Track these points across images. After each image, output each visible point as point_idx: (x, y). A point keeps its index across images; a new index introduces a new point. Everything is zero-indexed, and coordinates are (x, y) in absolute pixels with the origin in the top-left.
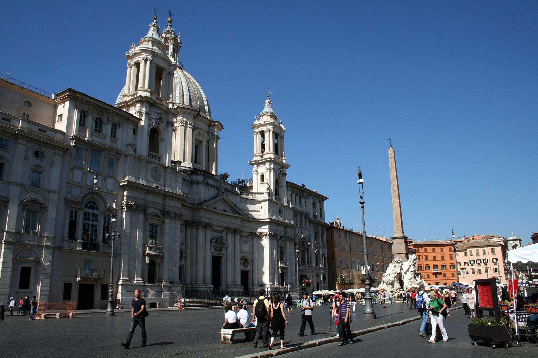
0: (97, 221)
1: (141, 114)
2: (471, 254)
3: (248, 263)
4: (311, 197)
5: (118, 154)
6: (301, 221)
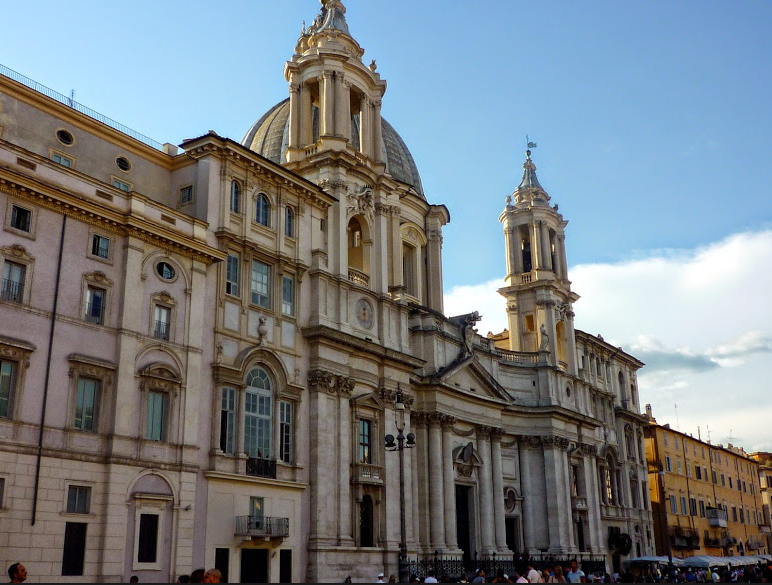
4: (615, 362)
5: (299, 268)
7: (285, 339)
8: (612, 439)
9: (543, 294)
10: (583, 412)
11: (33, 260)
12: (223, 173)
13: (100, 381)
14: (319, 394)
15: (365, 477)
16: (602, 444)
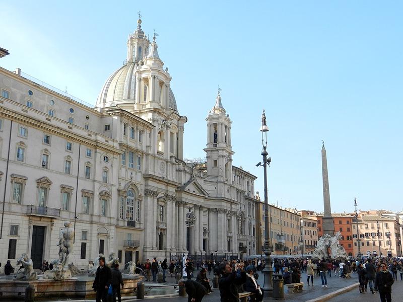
2: (367, 228)
5: (143, 153)
6: (240, 198)
8: (243, 209)
9: (221, 153)
12: (121, 121)
13: (89, 197)
15: (161, 226)
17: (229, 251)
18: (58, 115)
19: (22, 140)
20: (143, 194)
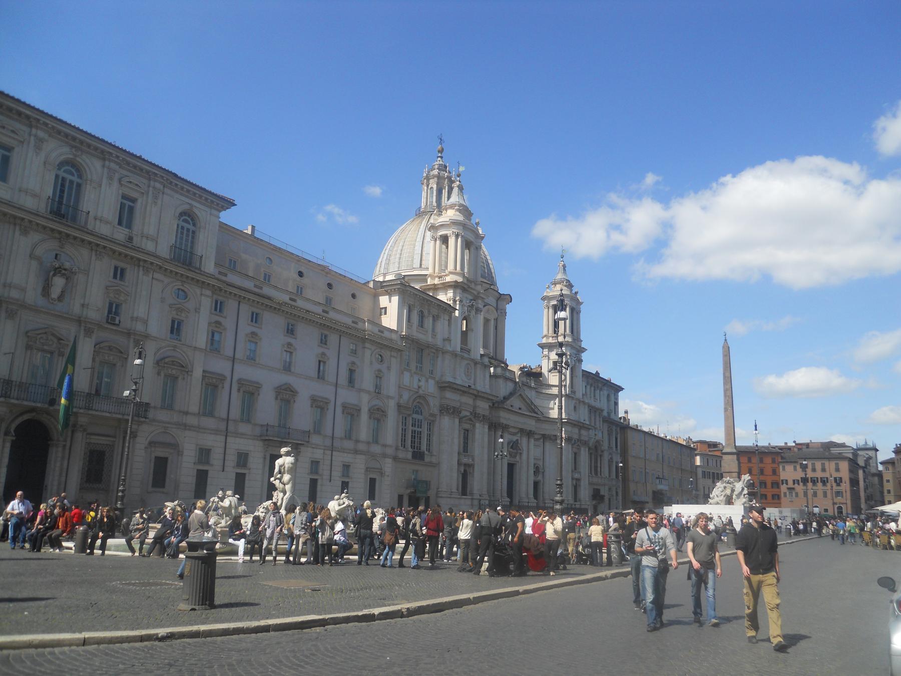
0: (421, 428)
1: (455, 301)
3: (539, 472)
5: (438, 350)
6: (595, 419)
7: (430, 387)
10: (582, 421)
11: (328, 359)
13: (353, 415)
14: (446, 417)
15: (465, 460)
16: (593, 440)
17: (576, 501)
18: (309, 293)
19: (254, 330)
20: (436, 411)
